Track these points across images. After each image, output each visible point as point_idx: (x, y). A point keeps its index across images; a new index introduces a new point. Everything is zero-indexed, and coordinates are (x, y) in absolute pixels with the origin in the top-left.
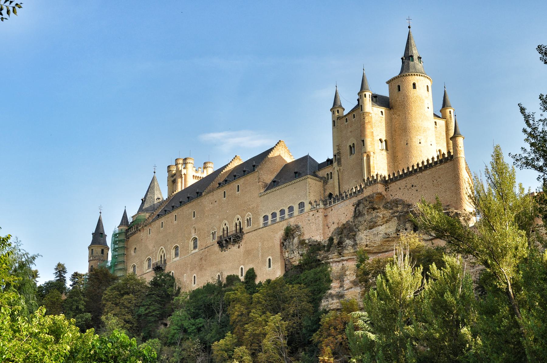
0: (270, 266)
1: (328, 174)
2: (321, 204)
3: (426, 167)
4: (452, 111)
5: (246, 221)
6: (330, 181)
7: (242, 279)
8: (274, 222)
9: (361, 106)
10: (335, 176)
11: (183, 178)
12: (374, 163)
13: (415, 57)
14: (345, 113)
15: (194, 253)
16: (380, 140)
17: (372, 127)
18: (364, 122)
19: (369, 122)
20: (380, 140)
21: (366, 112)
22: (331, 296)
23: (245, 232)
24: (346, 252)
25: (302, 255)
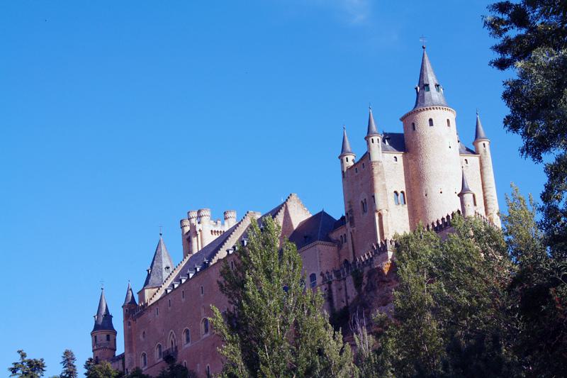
4: (487, 143)
6: (345, 245)
11: (199, 236)
12: (387, 222)
13: (432, 86)
15: (207, 338)
16: (396, 192)
17: (383, 179)
18: (373, 173)
19: (379, 173)
20: (396, 192)
21: (375, 162)
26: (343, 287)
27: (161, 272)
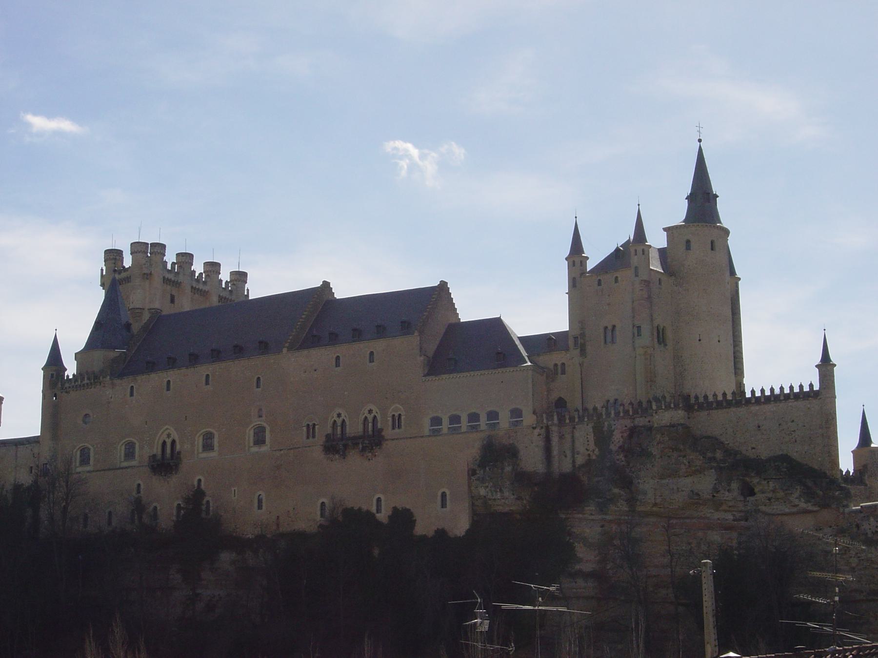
0: (444, 505)
1: (556, 365)
2: (555, 417)
5: (390, 419)
7: (383, 516)
8: (454, 431)
9: (636, 268)
14: (590, 265)
22: (581, 574)
23: (386, 437)
24: (612, 507)
25: (519, 498)
26: (568, 437)
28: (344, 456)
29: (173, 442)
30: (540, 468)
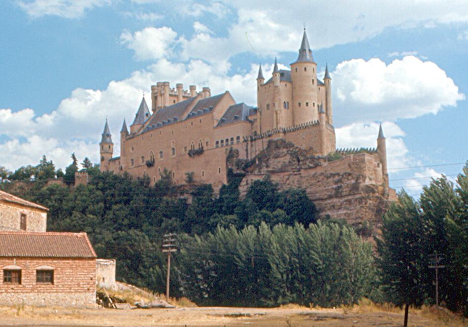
0: (220, 172)
3: (306, 127)
6: (255, 124)
10: (258, 121)
11: (163, 97)
16: (285, 102)
17: (280, 95)
27: (143, 117)
28: (194, 158)
29: (153, 156)
30: (245, 158)
